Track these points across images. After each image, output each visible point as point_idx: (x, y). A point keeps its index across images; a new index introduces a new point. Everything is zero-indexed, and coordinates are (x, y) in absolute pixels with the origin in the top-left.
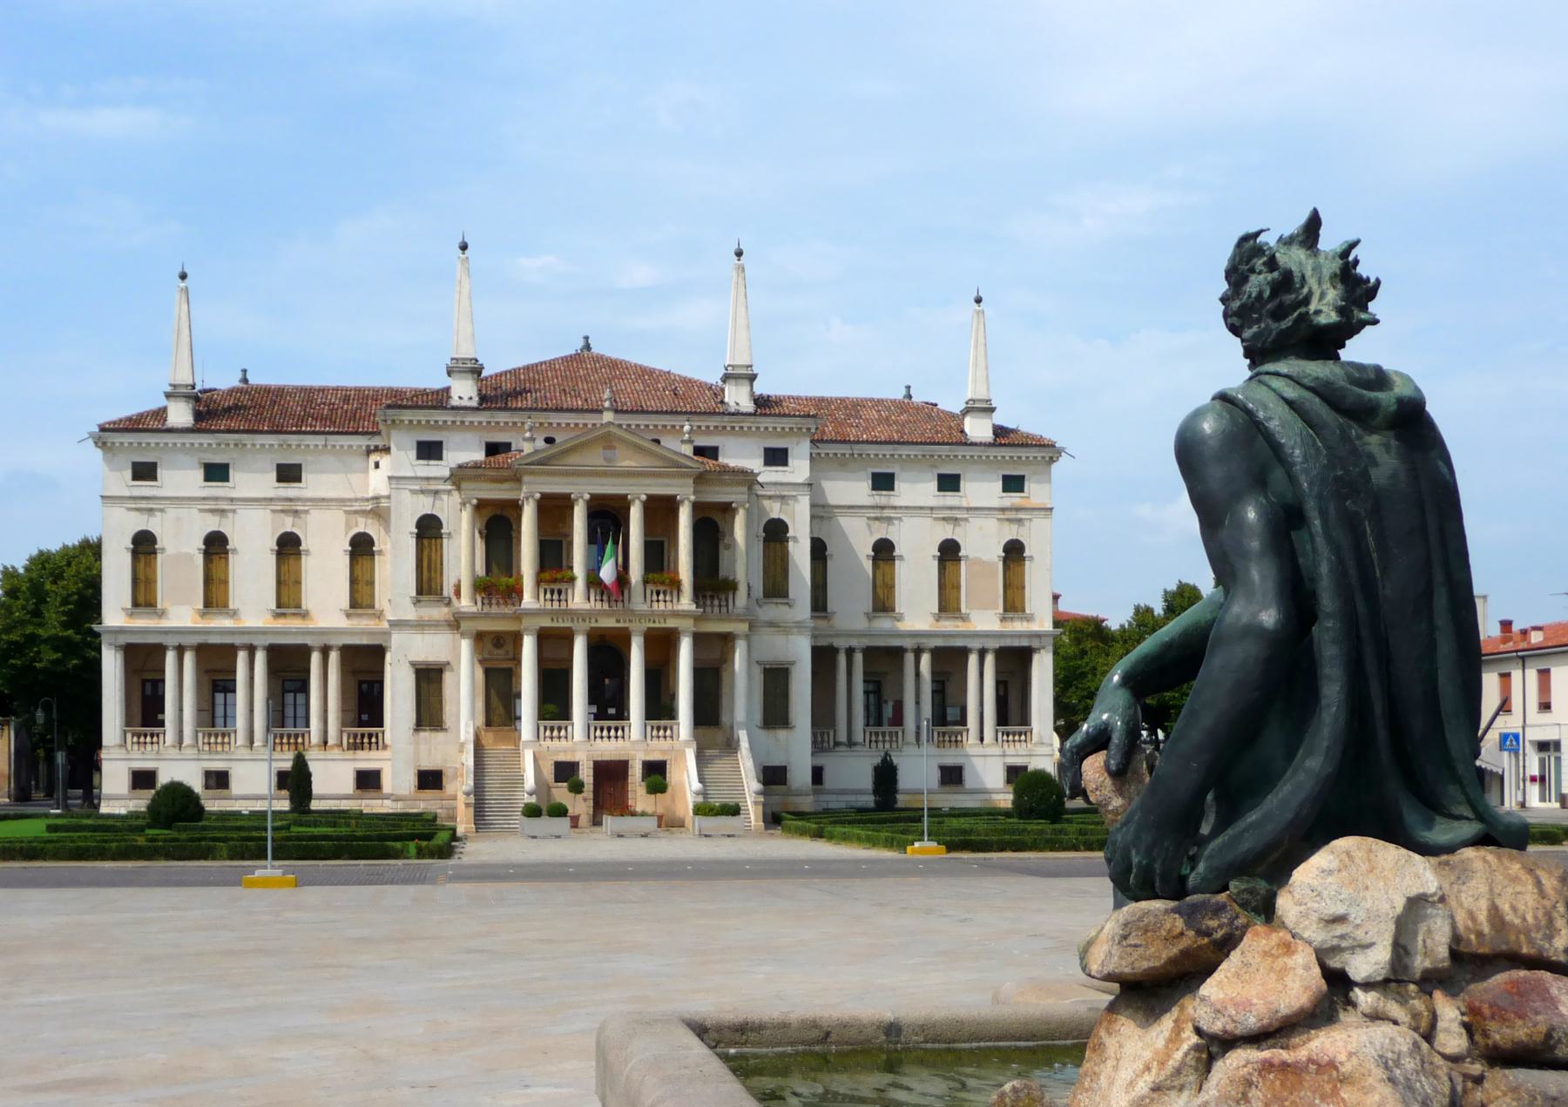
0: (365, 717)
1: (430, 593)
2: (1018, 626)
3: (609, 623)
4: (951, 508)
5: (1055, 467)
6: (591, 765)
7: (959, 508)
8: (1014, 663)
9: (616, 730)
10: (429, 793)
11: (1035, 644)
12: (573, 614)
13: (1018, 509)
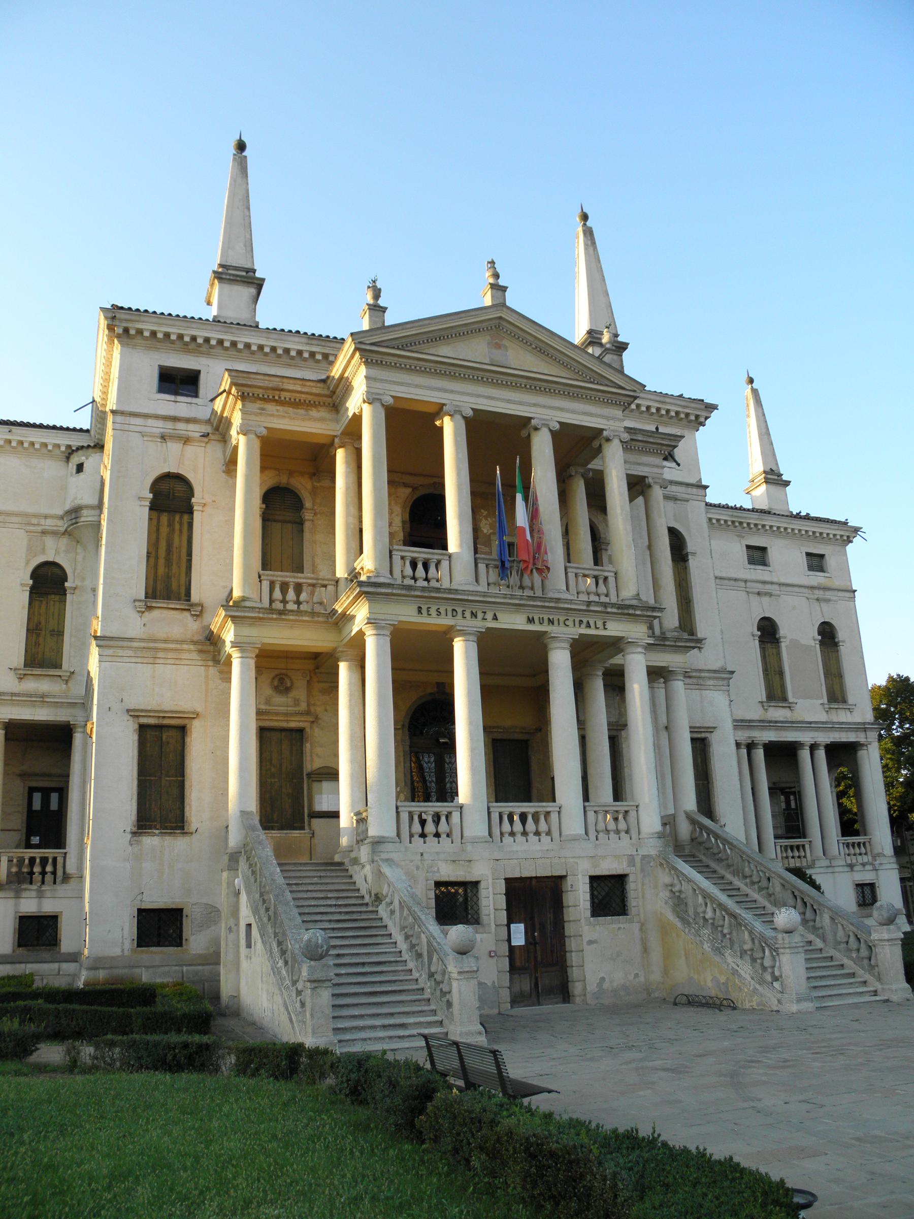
0: (35, 840)
1: (168, 595)
2: (842, 717)
3: (515, 621)
4: (764, 582)
5: (849, 547)
6: (502, 887)
7: (772, 583)
8: (842, 755)
9: (536, 820)
10: (156, 954)
11: (860, 737)
12: (455, 600)
13: (826, 589)
